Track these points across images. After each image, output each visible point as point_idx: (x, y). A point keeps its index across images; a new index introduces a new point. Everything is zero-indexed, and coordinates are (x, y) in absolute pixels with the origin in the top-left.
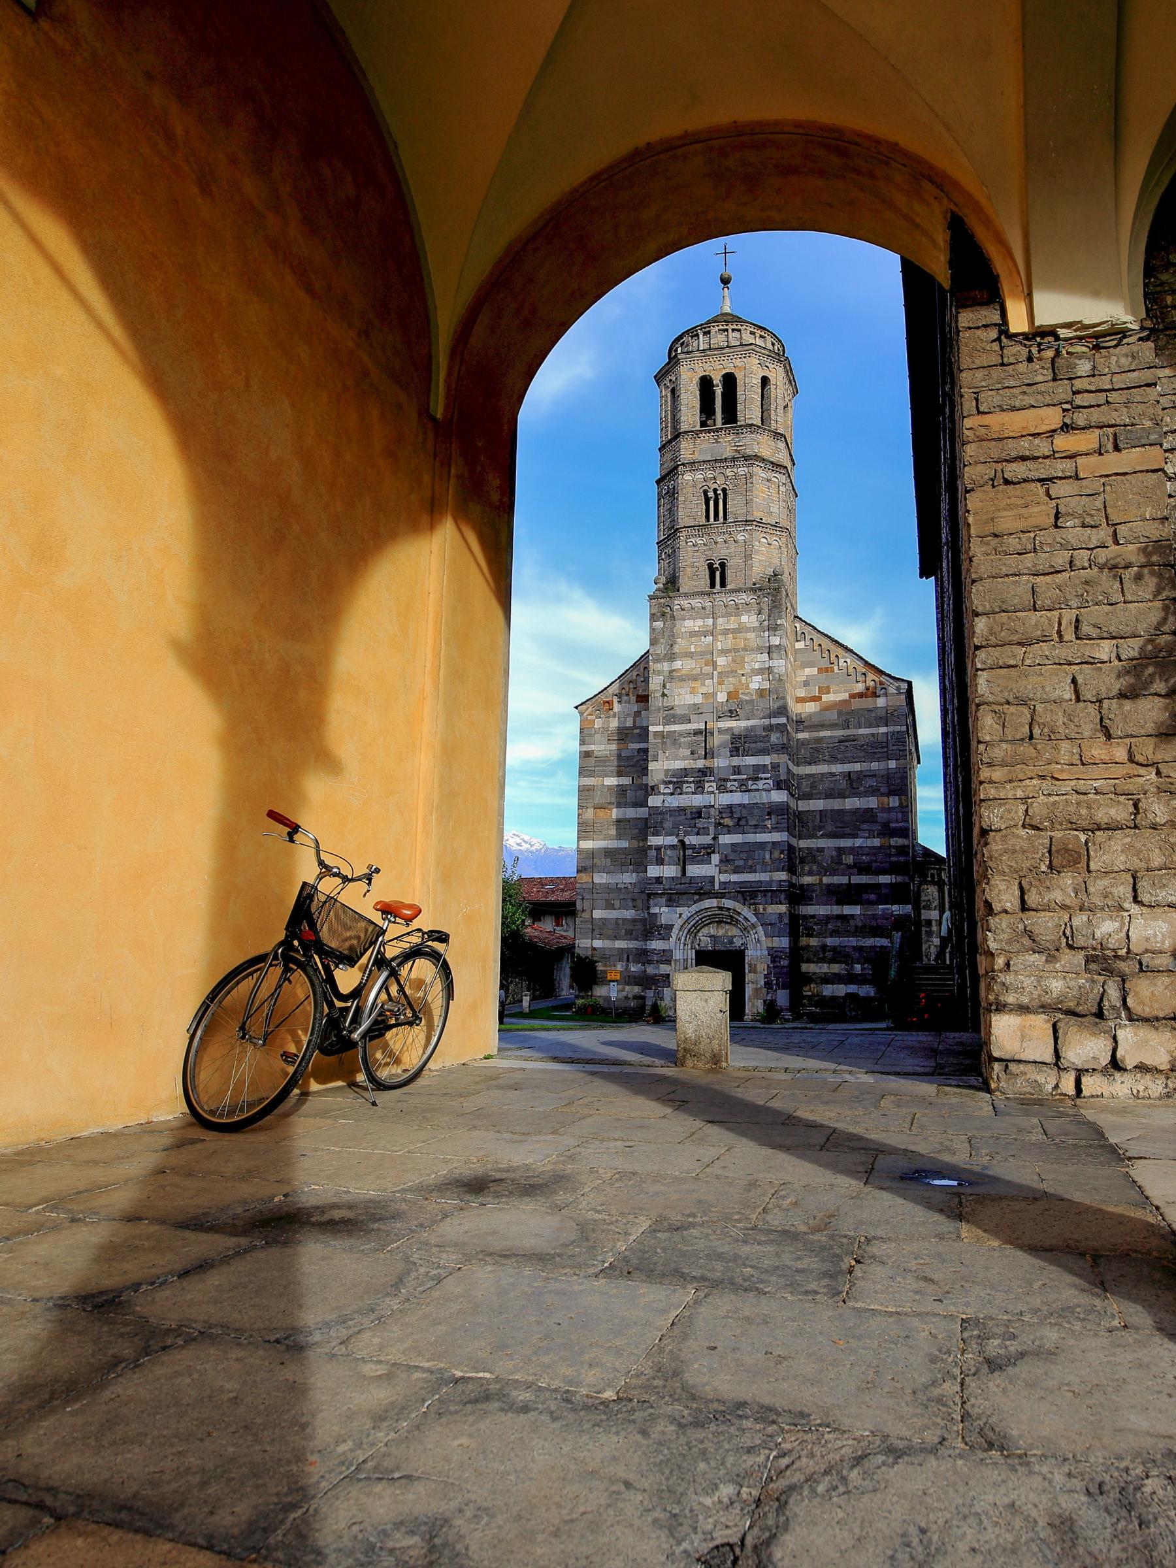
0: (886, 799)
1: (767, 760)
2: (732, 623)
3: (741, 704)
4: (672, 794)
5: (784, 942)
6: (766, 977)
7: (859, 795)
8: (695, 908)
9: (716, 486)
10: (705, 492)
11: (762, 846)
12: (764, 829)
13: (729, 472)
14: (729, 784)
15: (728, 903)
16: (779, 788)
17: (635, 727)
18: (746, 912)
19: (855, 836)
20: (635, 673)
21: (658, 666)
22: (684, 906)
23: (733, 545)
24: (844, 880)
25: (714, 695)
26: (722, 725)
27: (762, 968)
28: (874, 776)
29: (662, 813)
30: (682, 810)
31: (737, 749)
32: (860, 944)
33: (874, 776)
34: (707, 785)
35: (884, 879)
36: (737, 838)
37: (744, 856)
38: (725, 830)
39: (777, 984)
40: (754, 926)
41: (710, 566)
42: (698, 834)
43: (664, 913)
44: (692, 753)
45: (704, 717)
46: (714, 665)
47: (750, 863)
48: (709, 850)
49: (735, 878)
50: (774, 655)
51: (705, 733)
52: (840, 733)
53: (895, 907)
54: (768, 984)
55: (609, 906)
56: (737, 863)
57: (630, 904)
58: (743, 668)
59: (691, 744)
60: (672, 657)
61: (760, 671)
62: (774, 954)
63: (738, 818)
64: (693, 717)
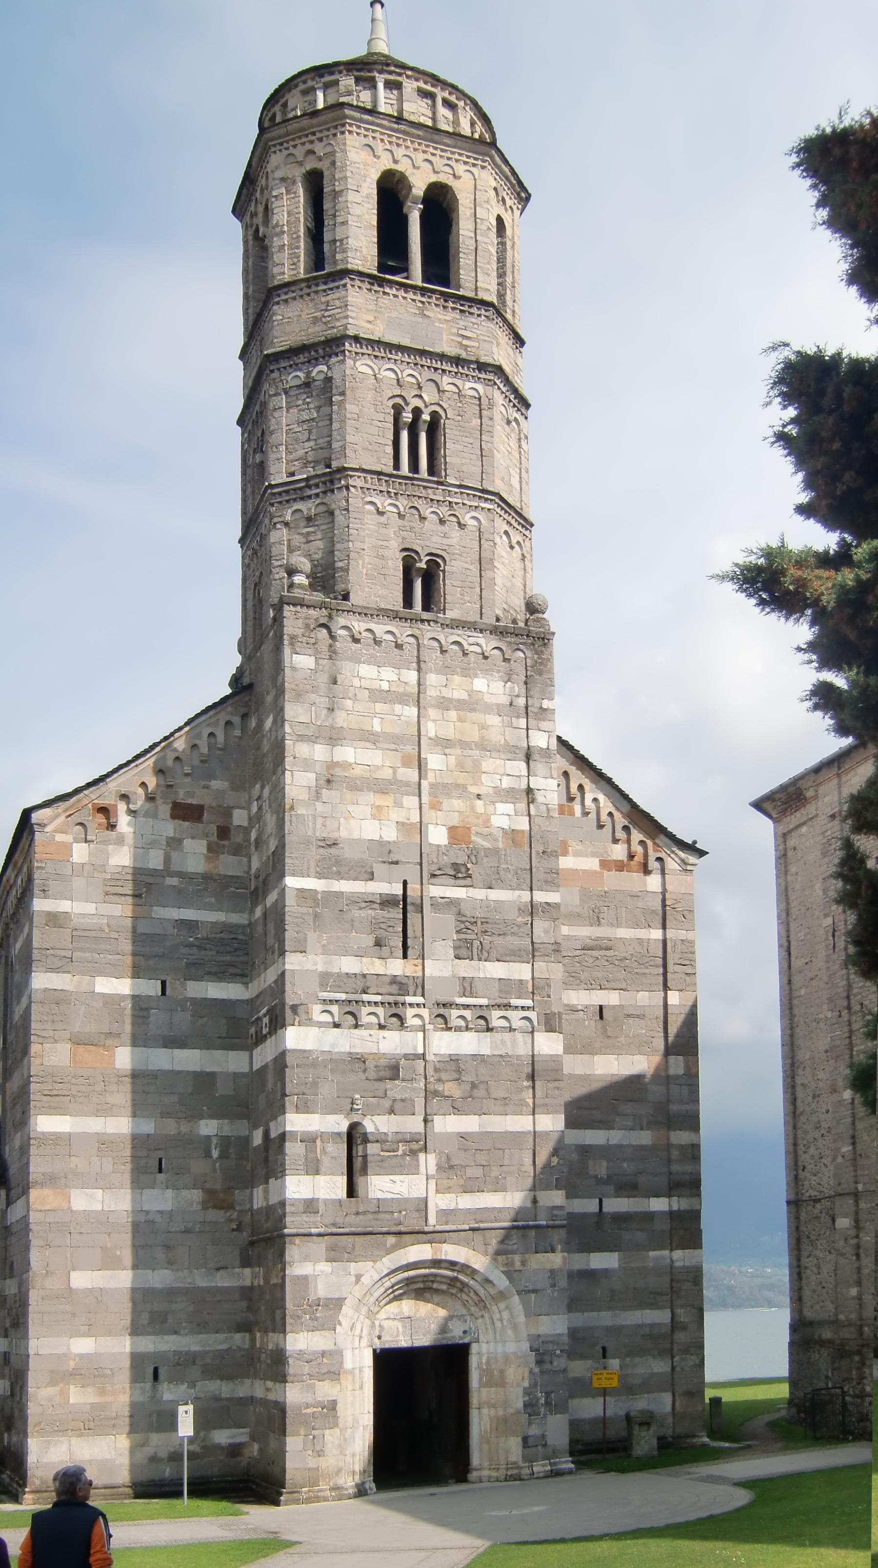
1: (522, 971)
3: (474, 854)
6: (526, 1392)
13: (445, 381)
14: (455, 1013)
16: (550, 1029)
17: (168, 871)
22: (365, 1258)
25: (421, 828)
26: (435, 891)
27: (518, 1378)
29: (314, 1064)
30: (359, 1060)
34: (410, 1012)
36: (469, 1123)
37: (482, 1158)
39: (547, 1403)
40: (502, 1295)
42: (392, 1111)
44: (378, 944)
46: (421, 765)
47: (495, 1172)
48: (418, 1144)
49: (467, 1202)
52: (585, 932)
54: (530, 1406)
56: (470, 1172)
57: (160, 1255)
58: (477, 782)
59: (375, 925)
60: (334, 738)
61: (509, 795)
62: (542, 1352)
63: (467, 1083)
64: (379, 869)
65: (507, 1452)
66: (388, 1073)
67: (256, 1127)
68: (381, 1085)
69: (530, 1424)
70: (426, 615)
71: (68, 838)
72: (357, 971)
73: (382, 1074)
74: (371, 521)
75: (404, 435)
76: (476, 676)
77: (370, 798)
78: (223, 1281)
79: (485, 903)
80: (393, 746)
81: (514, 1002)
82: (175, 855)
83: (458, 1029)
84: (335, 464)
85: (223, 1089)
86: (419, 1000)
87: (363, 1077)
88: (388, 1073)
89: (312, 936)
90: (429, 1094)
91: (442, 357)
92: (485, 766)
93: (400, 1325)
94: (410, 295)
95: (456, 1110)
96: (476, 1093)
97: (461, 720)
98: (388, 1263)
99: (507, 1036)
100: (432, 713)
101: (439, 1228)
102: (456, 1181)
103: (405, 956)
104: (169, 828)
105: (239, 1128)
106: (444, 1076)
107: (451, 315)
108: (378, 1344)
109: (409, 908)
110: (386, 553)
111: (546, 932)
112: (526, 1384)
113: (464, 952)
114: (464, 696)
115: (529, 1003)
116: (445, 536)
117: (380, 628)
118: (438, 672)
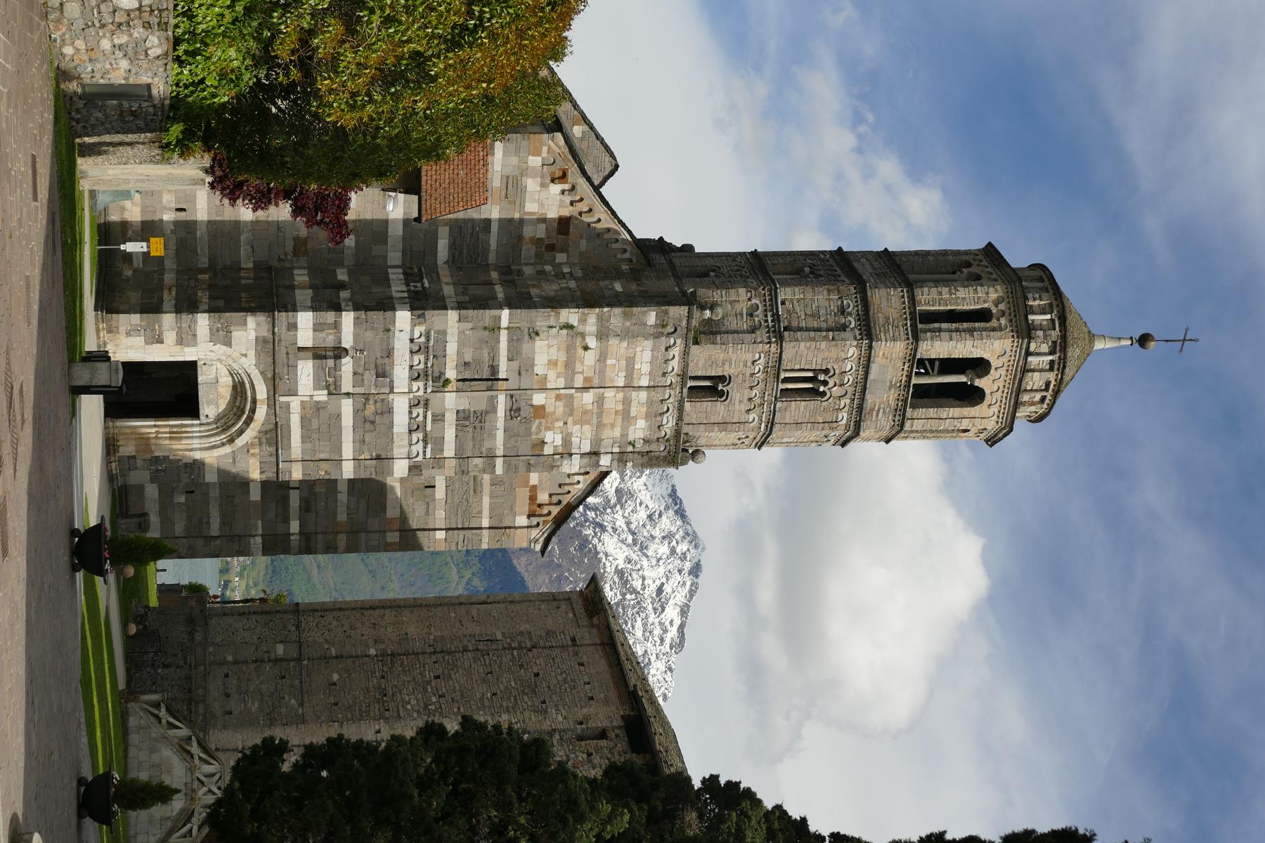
1: (449, 450)
3: (527, 421)
6: (166, 458)
9: (831, 384)
14: (421, 411)
15: (261, 412)
16: (410, 469)
23: (744, 407)
26: (502, 399)
28: (427, 513)
30: (389, 353)
31: (467, 418)
32: (212, 502)
33: (427, 513)
34: (421, 384)
35: (295, 526)
36: (347, 420)
37: (324, 428)
38: (360, 406)
41: (722, 379)
42: (355, 374)
44: (466, 364)
47: (315, 436)
48: (334, 390)
50: (586, 460)
53: (259, 540)
58: (575, 423)
59: (478, 362)
60: (602, 336)
61: (567, 441)
63: (374, 418)
64: (515, 364)
67: (350, 273)
68: (372, 366)
70: (685, 390)
72: (448, 352)
74: (749, 357)
75: (810, 374)
77: (562, 357)
78: (244, 251)
83: (410, 412)
84: (786, 333)
85: (377, 250)
86: (429, 390)
88: (380, 370)
89: (470, 325)
90: (367, 396)
91: (863, 399)
92: (586, 428)
94: (904, 378)
95: (356, 412)
99: (406, 442)
100: (620, 396)
105: (349, 260)
106: (379, 404)
107: (893, 403)
108: (199, 364)
113: (461, 415)
115: (428, 455)
116: (740, 402)
117: (675, 364)
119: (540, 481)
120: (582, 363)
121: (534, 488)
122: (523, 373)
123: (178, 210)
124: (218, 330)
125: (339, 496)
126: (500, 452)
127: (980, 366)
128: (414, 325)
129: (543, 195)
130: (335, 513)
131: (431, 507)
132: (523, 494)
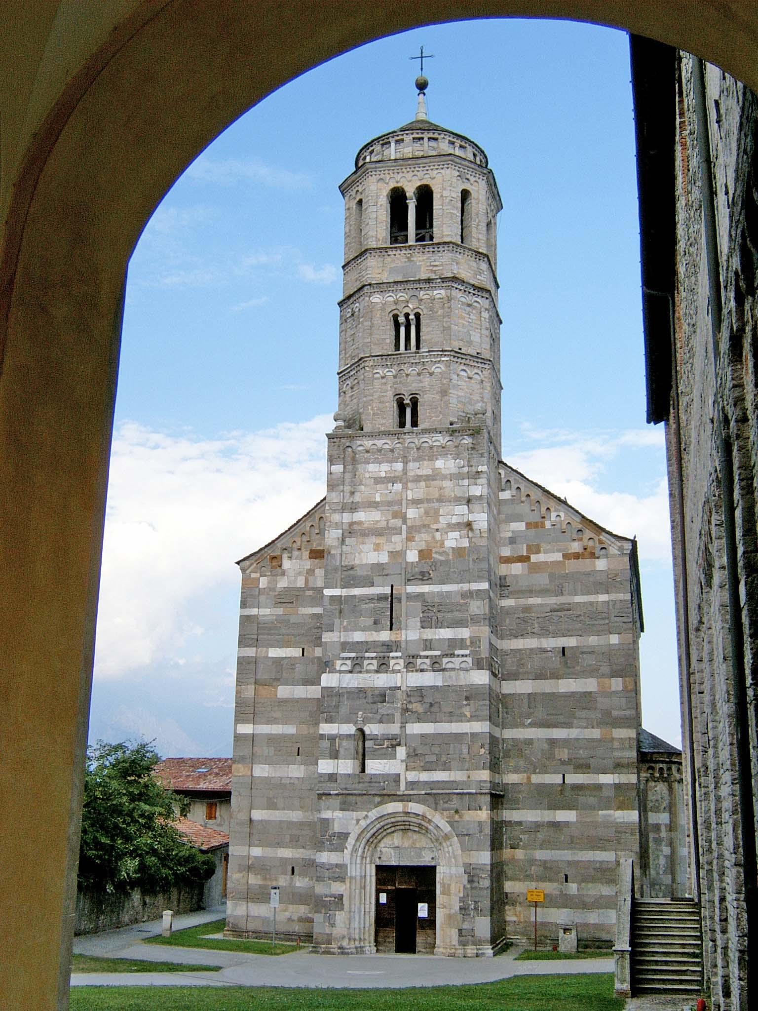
0: (606, 681)
2: (425, 470)
3: (435, 565)
4: (351, 672)
5: (484, 857)
6: (462, 900)
7: (576, 675)
8: (374, 814)
9: (406, 310)
10: (395, 317)
11: (458, 737)
12: (461, 718)
14: (419, 661)
15: (415, 807)
16: (480, 667)
17: (307, 588)
18: (440, 820)
19: (568, 725)
20: (308, 524)
21: (336, 517)
24: (557, 779)
25: (401, 554)
26: (411, 589)
30: (361, 692)
32: (576, 859)
34: (392, 662)
36: (428, 728)
39: (476, 909)
40: (447, 837)
42: (381, 721)
43: (338, 818)
45: (390, 580)
47: (444, 758)
48: (394, 742)
49: (424, 776)
51: (392, 598)
52: (553, 601)
53: (619, 813)
54: (463, 909)
55: (271, 805)
56: (428, 758)
58: (437, 521)
59: (374, 611)
60: (353, 508)
65: (450, 938)
66: (380, 699)
69: (464, 921)
71: (257, 575)
73: (377, 699)
76: (437, 459)
77: (374, 539)
79: (440, 594)
80: (387, 508)
81: (456, 652)
82: (311, 578)
83: (422, 671)
87: (365, 701)
88: (380, 699)
89: (337, 621)
92: (441, 512)
93: (392, 851)
95: (419, 720)
96: (433, 709)
97: (427, 487)
98: (374, 814)
101: (406, 792)
102: (419, 763)
103: (391, 629)
104: (308, 564)
109: (394, 600)
110: (385, 399)
111: (478, 608)
112: (462, 895)
114: (430, 472)
115: (467, 652)
116: (421, 381)
118: (414, 461)
119: (559, 551)
120: (377, 522)
121: (566, 556)
122: (386, 572)
123: (293, 873)
124: (332, 844)
125: (573, 736)
126: (465, 587)
127: (397, 198)
128: (333, 671)
129: (291, 573)
130: (593, 740)
131: (585, 650)
132: (573, 566)
